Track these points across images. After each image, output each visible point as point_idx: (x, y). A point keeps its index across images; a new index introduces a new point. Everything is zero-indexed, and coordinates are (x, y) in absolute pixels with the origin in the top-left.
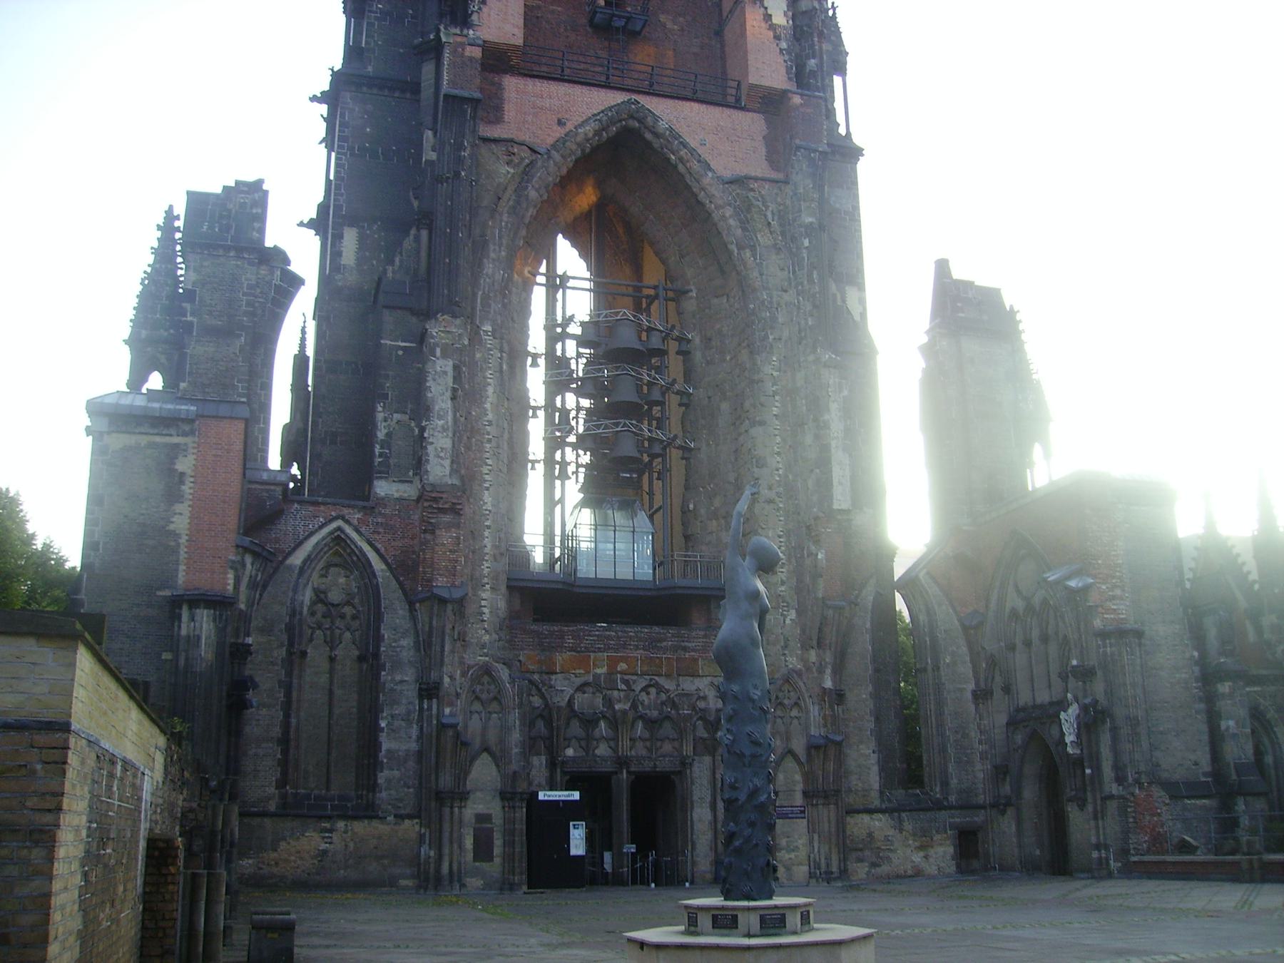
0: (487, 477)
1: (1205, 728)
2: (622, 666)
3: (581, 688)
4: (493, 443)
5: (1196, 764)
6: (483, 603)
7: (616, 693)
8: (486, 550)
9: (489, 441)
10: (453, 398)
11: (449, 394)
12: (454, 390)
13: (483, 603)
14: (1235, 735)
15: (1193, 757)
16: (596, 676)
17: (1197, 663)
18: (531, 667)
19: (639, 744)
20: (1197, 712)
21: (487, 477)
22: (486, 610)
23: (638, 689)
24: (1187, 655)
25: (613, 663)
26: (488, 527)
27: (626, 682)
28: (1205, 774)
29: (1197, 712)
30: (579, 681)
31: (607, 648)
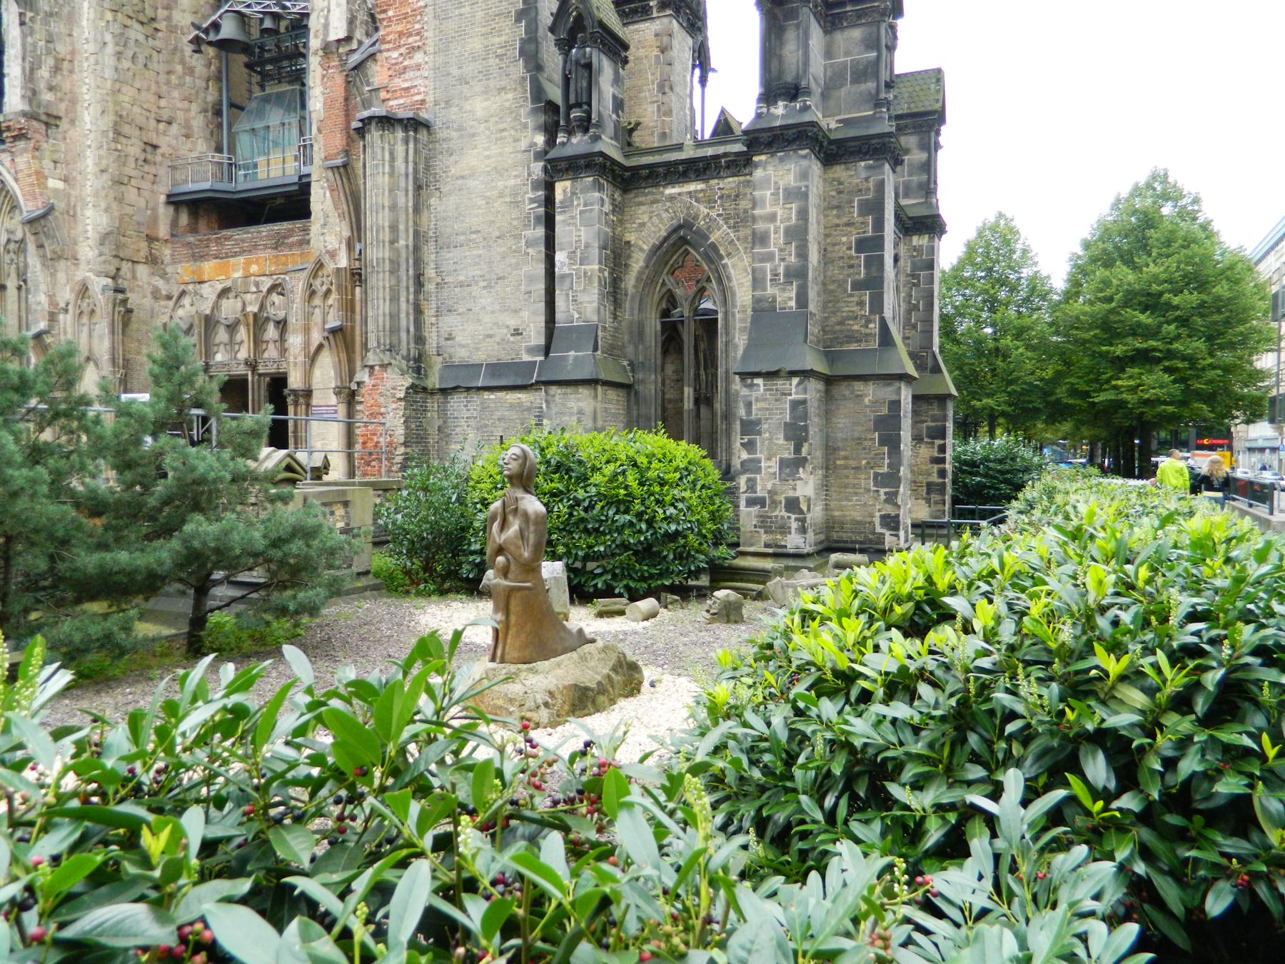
0: (86, 97)
1: (540, 269)
2: (254, 268)
3: (224, 293)
4: (92, 59)
5: (517, 332)
6: (88, 221)
7: (249, 296)
8: (89, 170)
9: (87, 59)
10: (22, 24)
11: (17, 21)
12: (21, 14)
13: (88, 221)
14: (563, 277)
15: (513, 322)
16: (235, 281)
17: (539, 156)
18: (187, 279)
19: (271, 346)
20: (528, 244)
21: (86, 97)
22: (89, 228)
23: (265, 290)
24: (524, 144)
25: (248, 264)
26: (89, 146)
27: (257, 284)
28: (531, 350)
29: (528, 244)
30: (219, 287)
31: (242, 252)
